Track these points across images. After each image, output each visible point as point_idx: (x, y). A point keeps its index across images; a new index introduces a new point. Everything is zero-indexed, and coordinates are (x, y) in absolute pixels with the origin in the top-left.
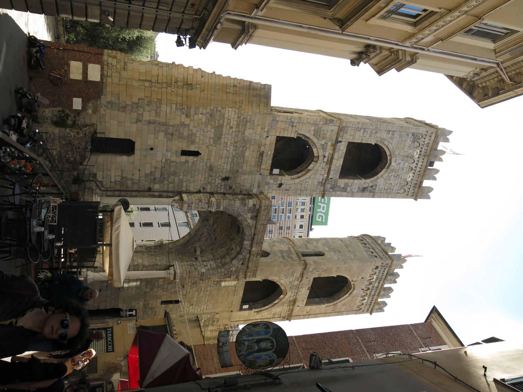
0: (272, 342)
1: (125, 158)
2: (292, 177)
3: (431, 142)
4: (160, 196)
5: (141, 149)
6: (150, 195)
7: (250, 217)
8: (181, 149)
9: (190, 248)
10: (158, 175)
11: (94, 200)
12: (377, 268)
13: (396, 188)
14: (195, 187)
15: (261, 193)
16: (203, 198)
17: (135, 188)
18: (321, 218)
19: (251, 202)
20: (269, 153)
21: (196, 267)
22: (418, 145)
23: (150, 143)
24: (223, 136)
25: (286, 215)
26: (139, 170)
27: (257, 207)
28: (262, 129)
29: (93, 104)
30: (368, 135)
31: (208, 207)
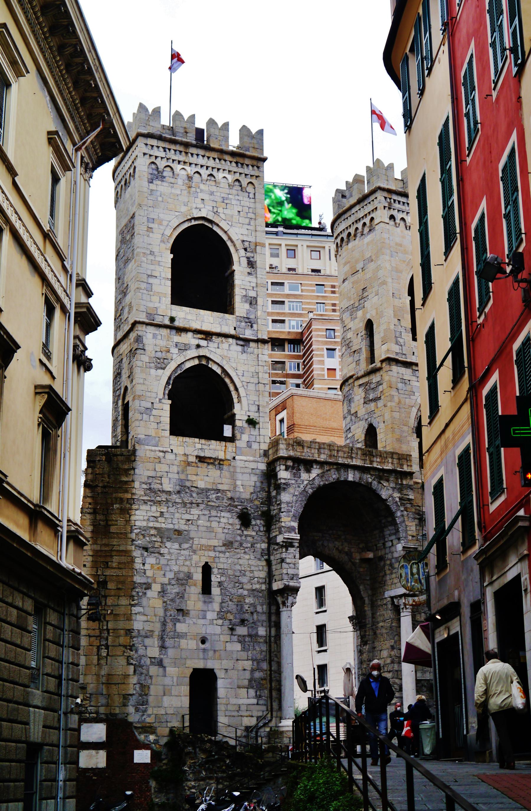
0: (413, 563)
1: (220, 683)
2: (235, 400)
3: (161, 144)
4: (278, 625)
5: (204, 659)
6: (276, 643)
7: (307, 474)
8: (201, 596)
9: (362, 570)
10: (242, 631)
11: (291, 729)
12: (392, 217)
13: (247, 202)
14: (261, 568)
15: (266, 454)
16: (278, 556)
17: (265, 666)
19: (283, 474)
20: (199, 446)
21: (393, 561)
22: (168, 169)
23: (192, 644)
24: (176, 527)
25: (288, 296)
26: (237, 660)
27: (290, 463)
28: (160, 462)
29: (140, 733)
30: (157, 268)
31: (293, 546)
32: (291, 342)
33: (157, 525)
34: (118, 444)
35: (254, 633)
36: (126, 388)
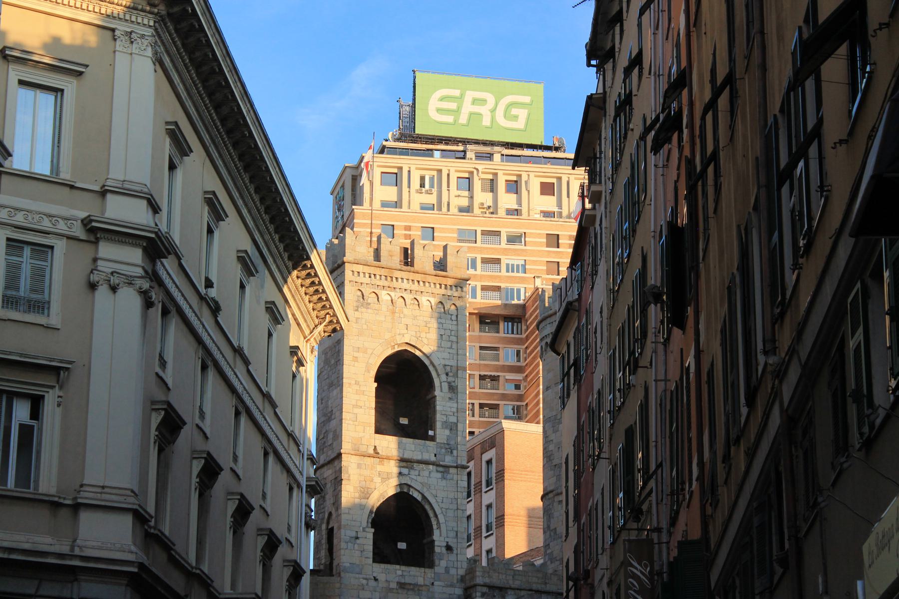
2: (435, 527)
3: (367, 270)
15: (462, 579)
18: (514, 111)
27: (485, 589)
32: (507, 319)
34: (322, 567)
36: (330, 514)
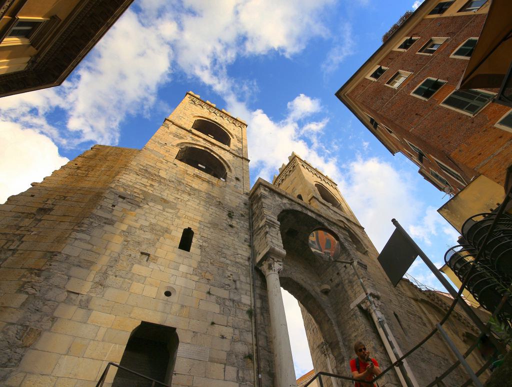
7: (280, 200)
10: (224, 294)
24: (165, 198)
26: (213, 323)
31: (275, 228)
33: (145, 189)
35: (235, 299)
